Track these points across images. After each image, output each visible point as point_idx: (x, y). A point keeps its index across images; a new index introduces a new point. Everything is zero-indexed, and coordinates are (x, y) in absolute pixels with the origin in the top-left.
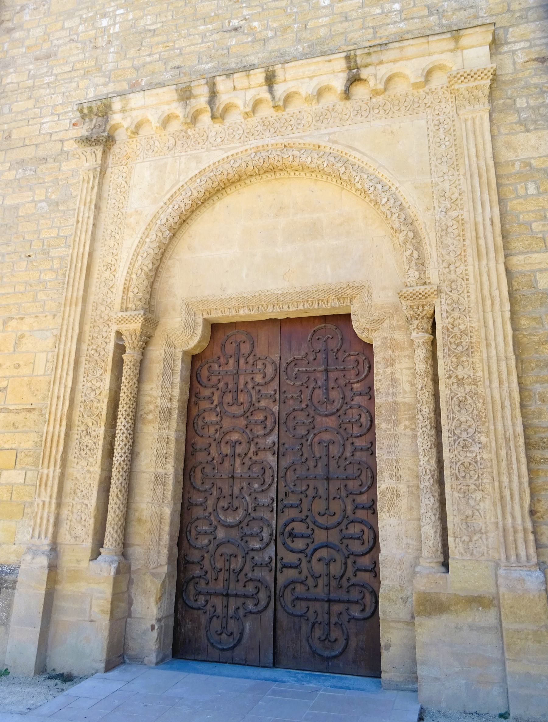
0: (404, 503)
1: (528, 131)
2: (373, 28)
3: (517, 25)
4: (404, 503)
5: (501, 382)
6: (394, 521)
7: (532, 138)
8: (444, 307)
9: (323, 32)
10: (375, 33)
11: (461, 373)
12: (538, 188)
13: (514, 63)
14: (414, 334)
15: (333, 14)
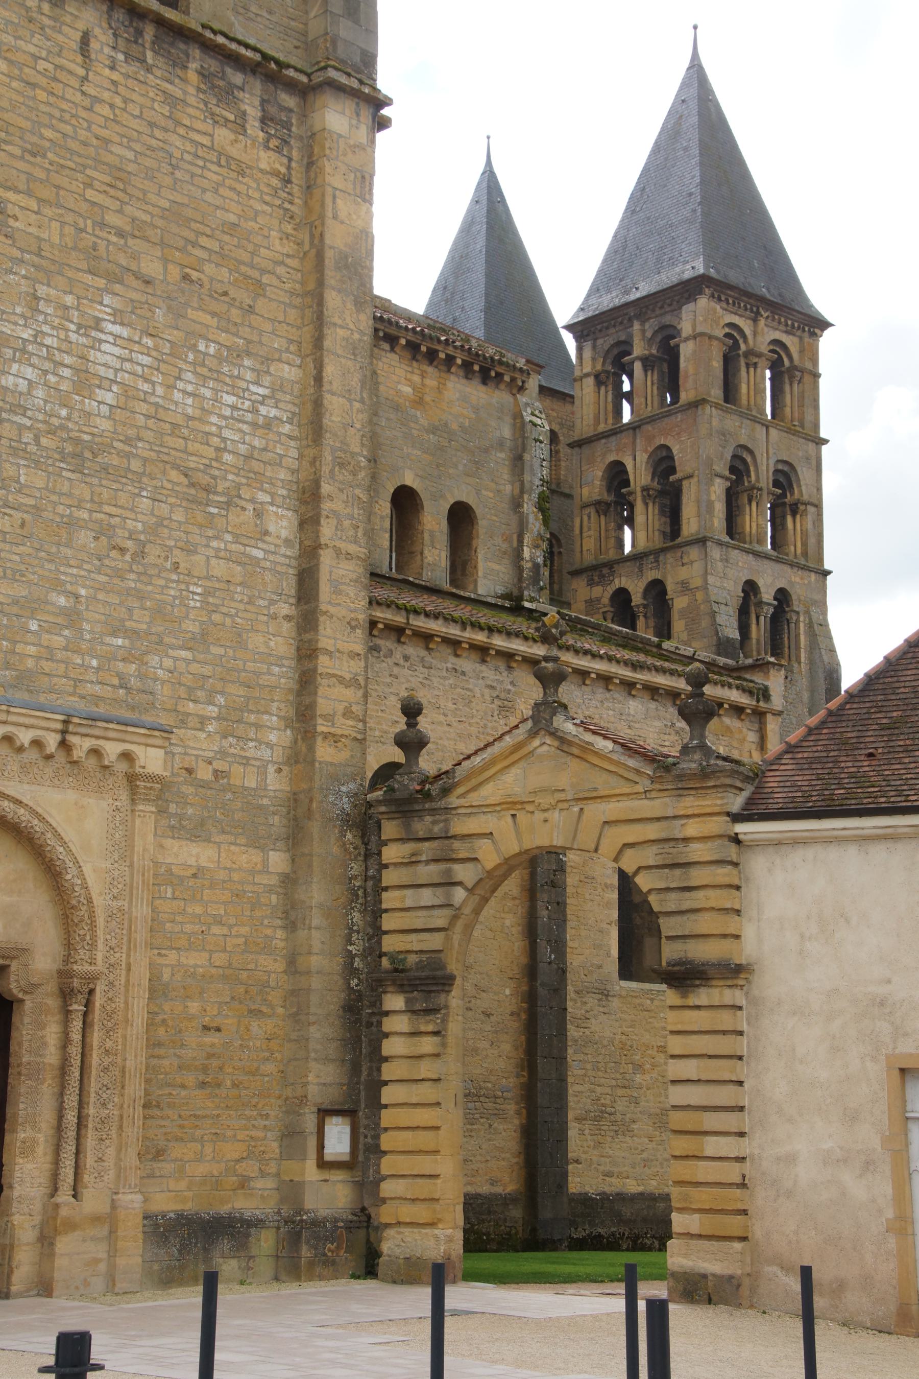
0: (40, 1150)
1: (173, 838)
2: (75, 680)
3: (180, 728)
4: (40, 1150)
5: (136, 1056)
6: (30, 1166)
7: (176, 843)
8: (104, 987)
9: (30, 663)
10: (75, 686)
11: (109, 1044)
12: (173, 893)
13: (173, 766)
14: (75, 1007)
15: (40, 645)
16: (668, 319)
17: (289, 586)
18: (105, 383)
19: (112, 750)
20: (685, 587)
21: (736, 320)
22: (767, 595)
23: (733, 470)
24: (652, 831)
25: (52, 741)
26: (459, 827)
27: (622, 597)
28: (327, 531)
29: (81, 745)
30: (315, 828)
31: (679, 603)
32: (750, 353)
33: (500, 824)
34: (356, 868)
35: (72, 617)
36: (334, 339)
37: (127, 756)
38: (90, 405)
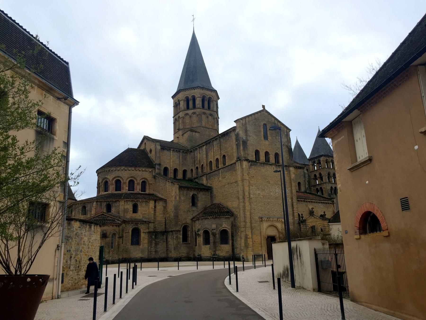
16: (319, 159)
17: (291, 205)
18: (277, 193)
19: (281, 220)
20: (324, 188)
21: (327, 158)
22: (334, 188)
23: (328, 174)
24: (322, 224)
25: (277, 220)
26: (307, 224)
27: (317, 189)
28: (294, 201)
29: (279, 220)
30: (295, 224)
31: (324, 190)
32: (329, 162)
33: (310, 224)
34: (299, 227)
35: (277, 210)
36: (293, 186)
37: (281, 220)
38: (276, 195)
